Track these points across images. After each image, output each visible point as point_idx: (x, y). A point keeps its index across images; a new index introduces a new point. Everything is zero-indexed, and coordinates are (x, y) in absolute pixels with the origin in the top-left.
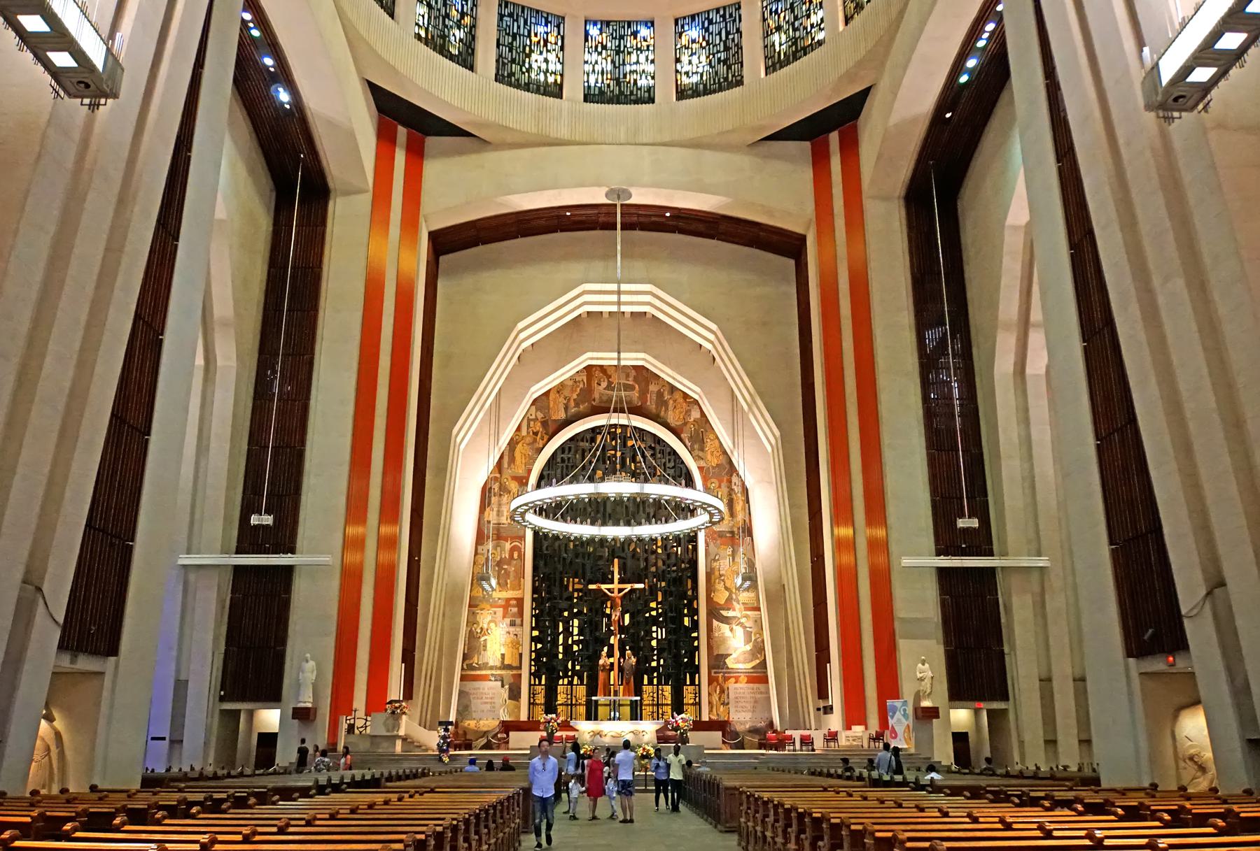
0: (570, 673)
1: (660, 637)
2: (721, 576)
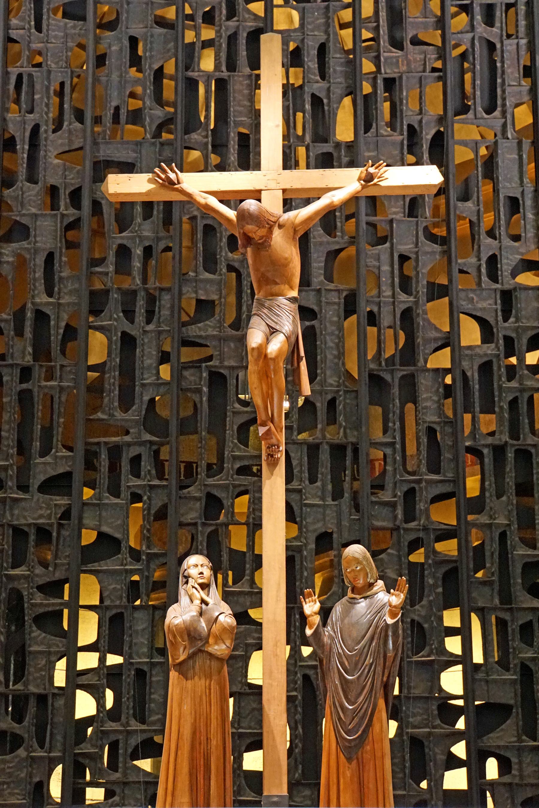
1: (478, 657)
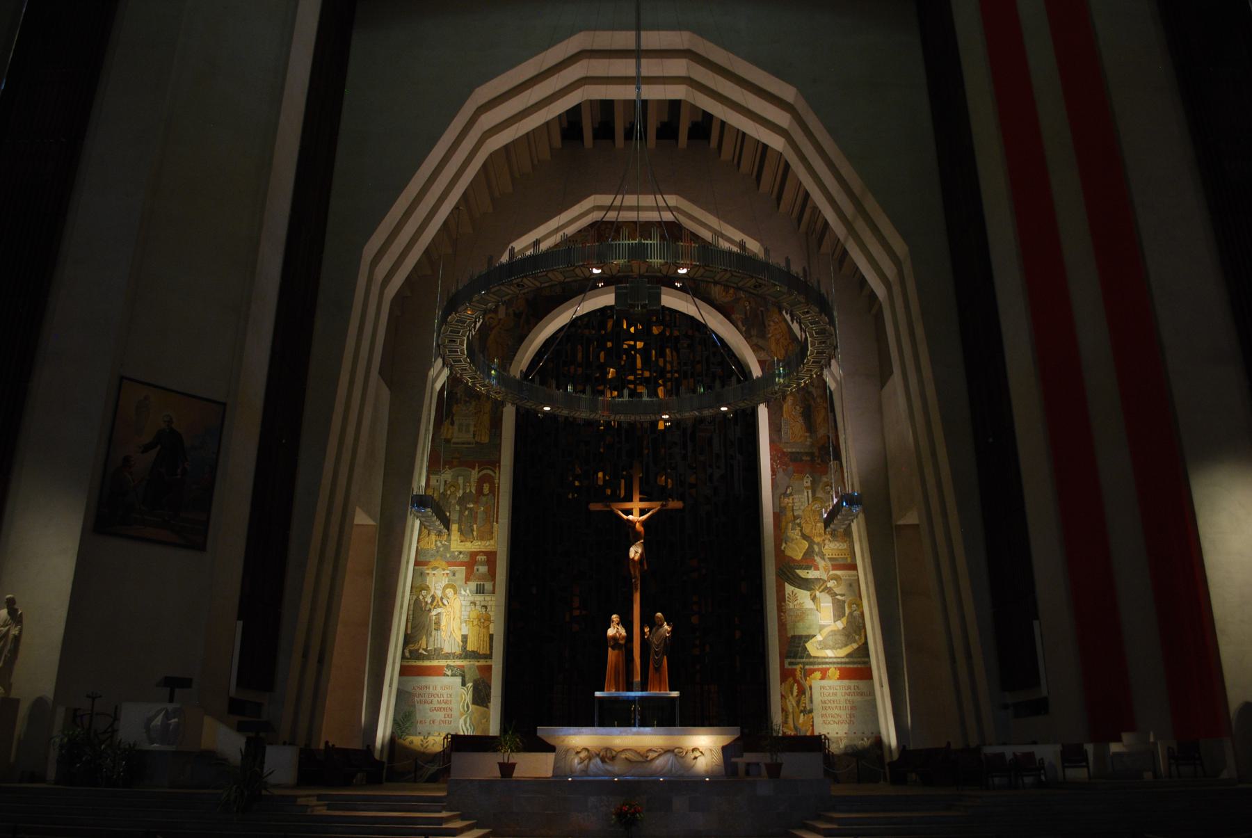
2: (795, 518)
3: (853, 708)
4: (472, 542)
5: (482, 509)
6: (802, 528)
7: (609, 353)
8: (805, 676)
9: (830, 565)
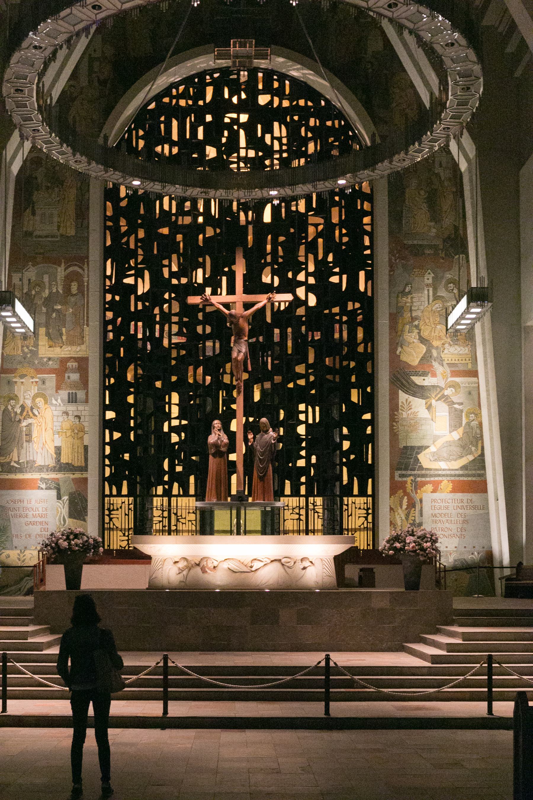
0: (166, 478)
2: (413, 319)
3: (465, 522)
4: (61, 347)
5: (71, 310)
6: (420, 330)
7: (208, 127)
8: (416, 489)
9: (449, 372)
